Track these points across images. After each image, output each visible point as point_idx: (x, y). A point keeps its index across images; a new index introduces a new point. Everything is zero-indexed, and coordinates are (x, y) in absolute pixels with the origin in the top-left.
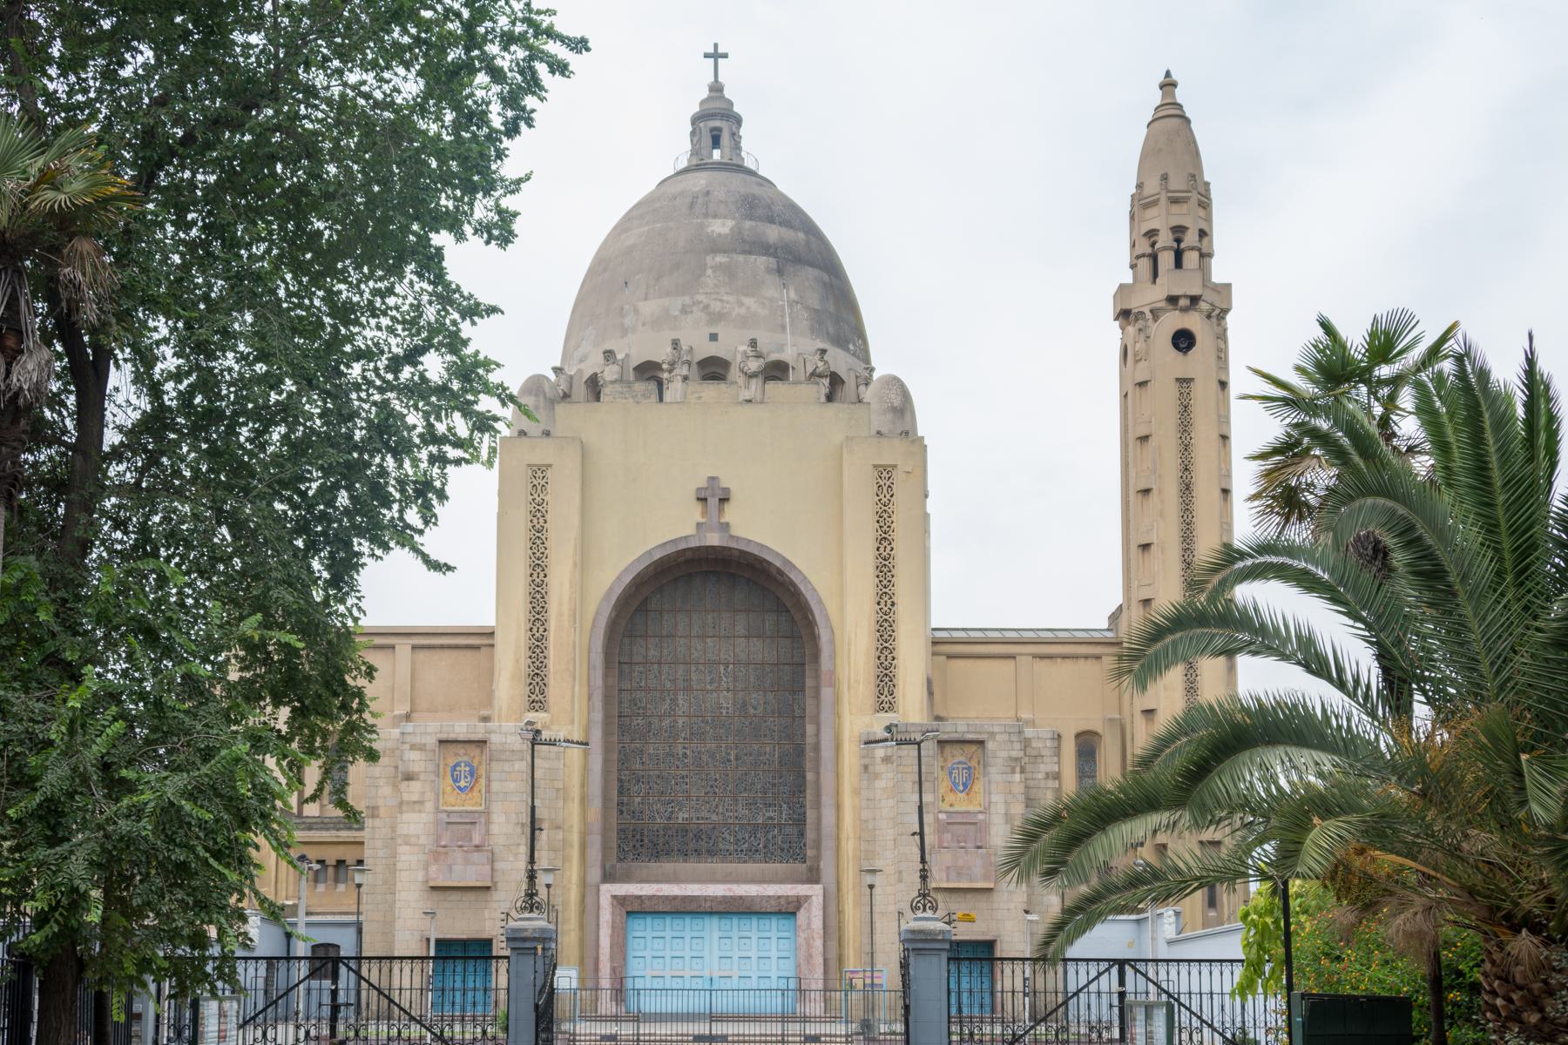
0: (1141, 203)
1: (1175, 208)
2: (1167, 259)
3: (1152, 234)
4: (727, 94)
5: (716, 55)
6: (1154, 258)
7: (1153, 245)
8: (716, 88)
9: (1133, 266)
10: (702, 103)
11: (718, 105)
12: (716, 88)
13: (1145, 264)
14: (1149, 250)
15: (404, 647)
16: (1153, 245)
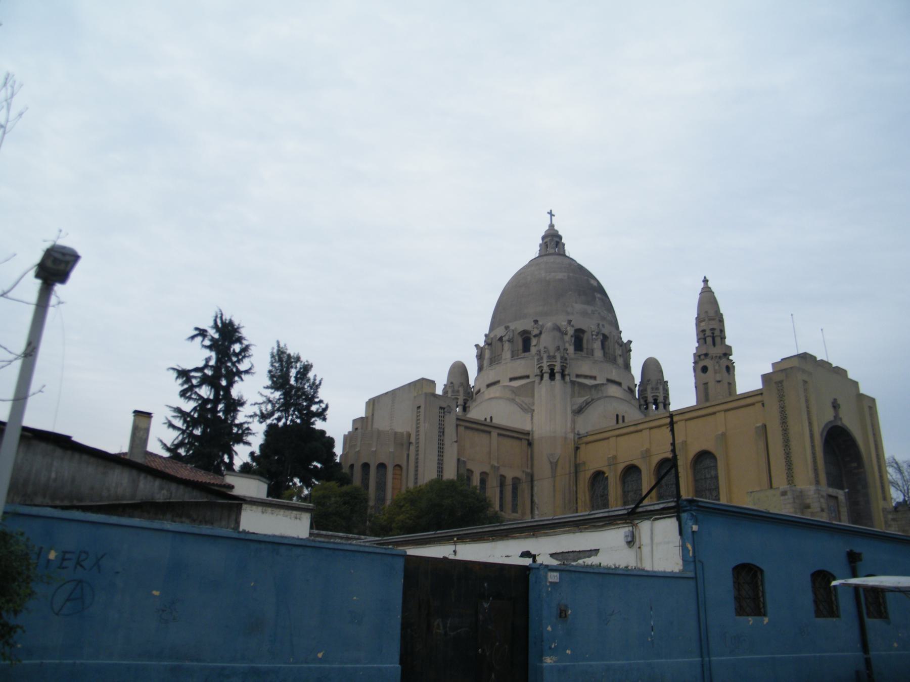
0: (699, 320)
1: (711, 322)
2: (709, 340)
3: (704, 331)
4: (556, 228)
5: (551, 214)
6: (705, 339)
7: (704, 335)
8: (552, 226)
9: (698, 342)
10: (546, 232)
11: (552, 232)
12: (552, 226)
13: (702, 341)
14: (703, 337)
15: (494, 434)
16: (704, 335)
